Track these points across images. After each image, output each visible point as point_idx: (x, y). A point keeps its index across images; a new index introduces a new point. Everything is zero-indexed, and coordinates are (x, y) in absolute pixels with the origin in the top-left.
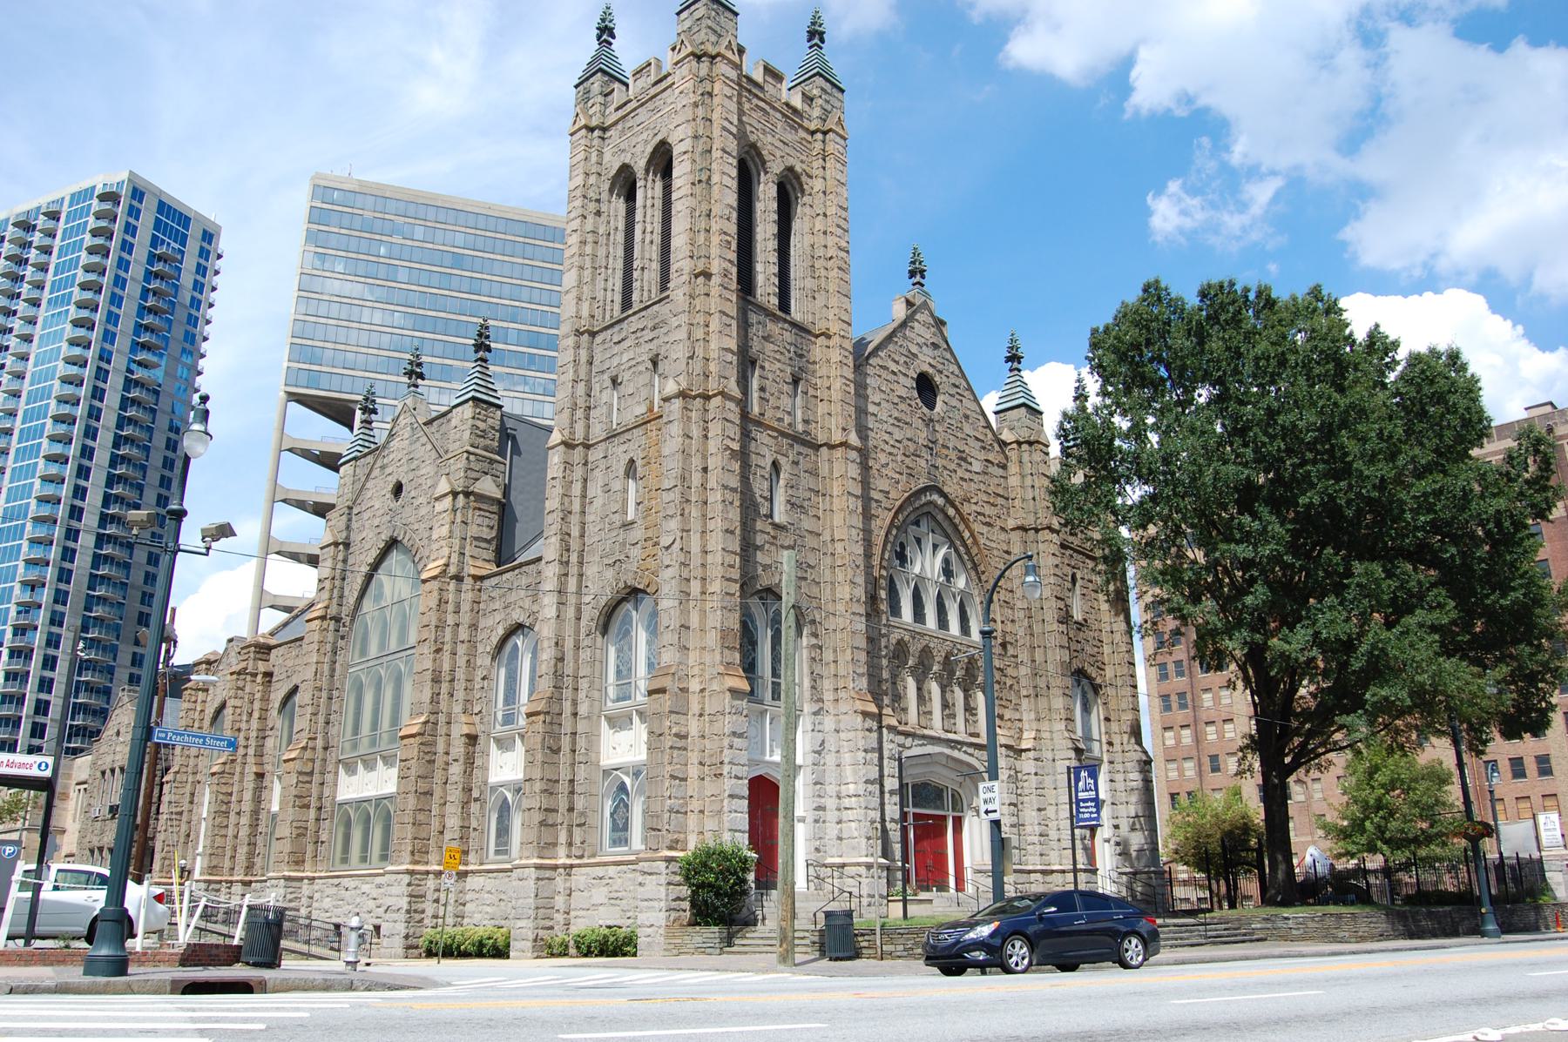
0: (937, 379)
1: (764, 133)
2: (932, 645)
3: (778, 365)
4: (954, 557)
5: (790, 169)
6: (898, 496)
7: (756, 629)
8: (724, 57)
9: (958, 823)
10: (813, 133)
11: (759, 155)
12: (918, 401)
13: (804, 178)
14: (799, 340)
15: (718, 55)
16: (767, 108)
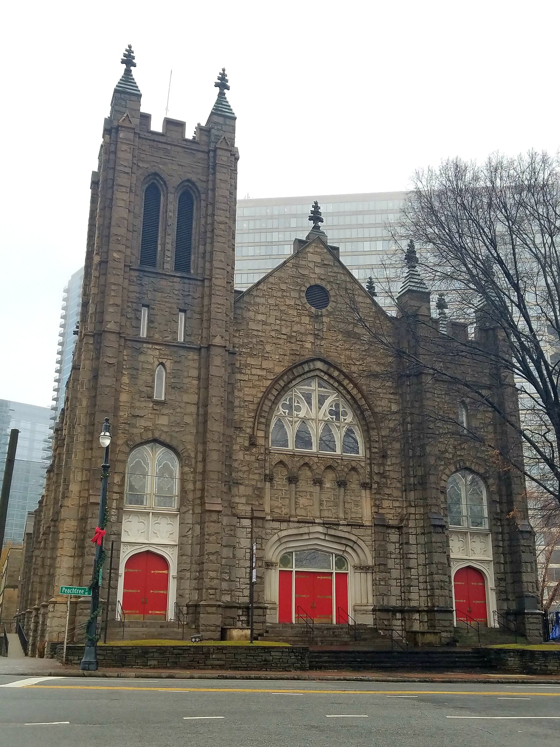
0: (328, 288)
1: (165, 164)
3: (169, 305)
4: (342, 401)
5: (189, 181)
6: (279, 370)
7: (147, 464)
8: (122, 127)
9: (342, 578)
10: (208, 153)
11: (162, 179)
12: (308, 306)
13: (199, 184)
14: (186, 286)
15: (119, 126)
16: (169, 147)
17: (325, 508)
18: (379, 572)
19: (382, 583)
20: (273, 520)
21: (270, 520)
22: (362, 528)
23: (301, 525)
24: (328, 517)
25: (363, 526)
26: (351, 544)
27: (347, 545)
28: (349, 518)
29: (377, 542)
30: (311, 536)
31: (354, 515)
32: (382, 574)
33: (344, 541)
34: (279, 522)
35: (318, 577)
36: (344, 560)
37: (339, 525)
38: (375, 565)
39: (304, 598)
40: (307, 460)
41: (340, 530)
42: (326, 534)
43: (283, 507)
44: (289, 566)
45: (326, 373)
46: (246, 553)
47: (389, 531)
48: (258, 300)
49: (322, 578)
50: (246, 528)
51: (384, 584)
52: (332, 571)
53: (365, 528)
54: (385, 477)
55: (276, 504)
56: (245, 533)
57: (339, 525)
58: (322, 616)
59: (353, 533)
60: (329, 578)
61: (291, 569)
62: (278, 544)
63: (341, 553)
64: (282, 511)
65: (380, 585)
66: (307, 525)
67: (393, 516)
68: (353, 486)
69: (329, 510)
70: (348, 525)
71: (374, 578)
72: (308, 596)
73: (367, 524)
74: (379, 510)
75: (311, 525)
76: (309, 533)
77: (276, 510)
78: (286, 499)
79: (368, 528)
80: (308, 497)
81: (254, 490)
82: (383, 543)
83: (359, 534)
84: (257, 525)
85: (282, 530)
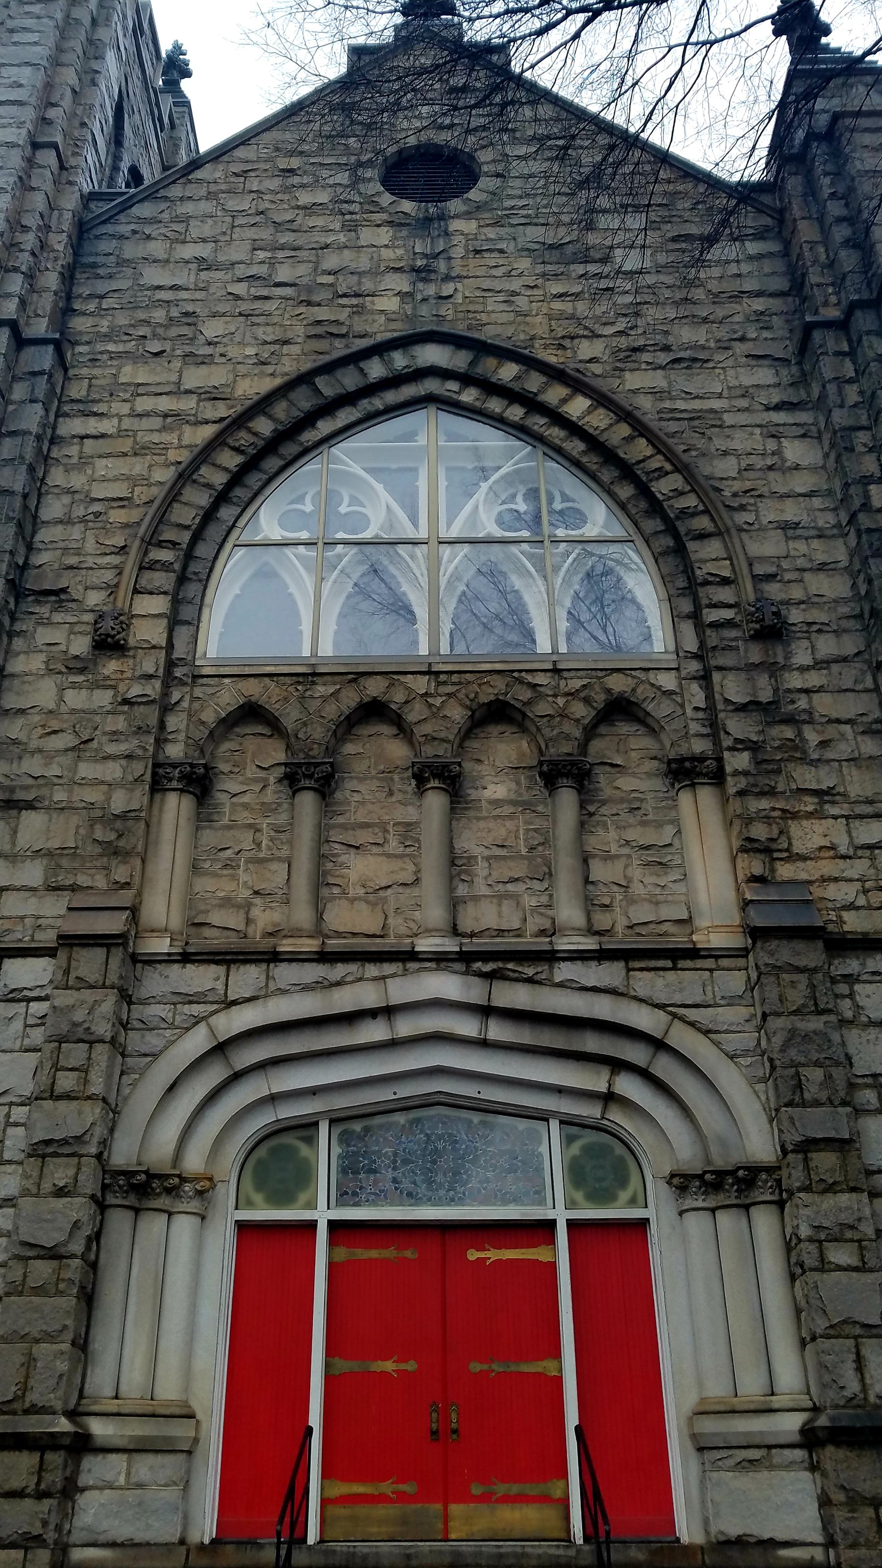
2: (399, 697)
17: (484, 890)
18: (807, 1189)
19: (840, 1255)
20: (186, 958)
21: (168, 960)
22: (688, 963)
23: (340, 970)
24: (501, 932)
25: (694, 953)
26: (636, 1054)
27: (617, 1065)
28: (619, 929)
29: (775, 1023)
30: (405, 1027)
31: (642, 913)
32: (829, 1202)
33: (592, 1043)
34: (217, 963)
35: (473, 1255)
36: (620, 1149)
37: (551, 957)
38: (785, 1152)
39: (384, 1374)
40: (374, 688)
41: (561, 985)
42: (486, 1011)
43: (258, 901)
44: (303, 1197)
45: (466, 380)
46: (8, 1124)
47: (852, 965)
48: (188, 208)
49: (493, 1255)
50: (29, 1000)
51: (854, 1261)
52: (550, 1215)
53: (710, 963)
54: (790, 720)
55: (223, 887)
56: (17, 1025)
57: (551, 957)
58: (501, 1489)
59: (641, 993)
60: (540, 1254)
61: (306, 1215)
62: (214, 1075)
63: (590, 1111)
64: (248, 921)
65: (824, 1266)
66: (372, 970)
67: (865, 892)
68: (626, 783)
69: (500, 898)
70: (602, 955)
71: (789, 1231)
72: (411, 1366)
73: (717, 940)
74: (773, 870)
75: (389, 968)
76: (388, 1012)
77: (216, 918)
78: (274, 866)
79: (724, 962)
80: (393, 845)
81: (93, 822)
82: (815, 1024)
83: (678, 999)
84: (72, 975)
85: (234, 1003)
